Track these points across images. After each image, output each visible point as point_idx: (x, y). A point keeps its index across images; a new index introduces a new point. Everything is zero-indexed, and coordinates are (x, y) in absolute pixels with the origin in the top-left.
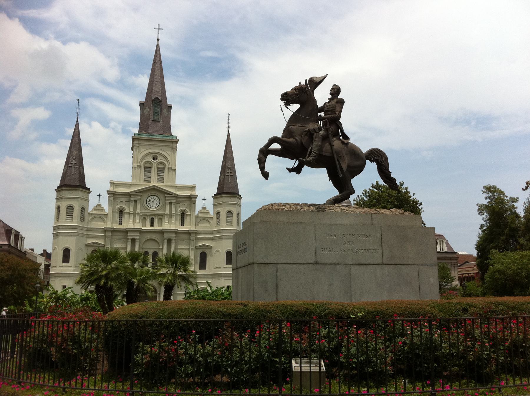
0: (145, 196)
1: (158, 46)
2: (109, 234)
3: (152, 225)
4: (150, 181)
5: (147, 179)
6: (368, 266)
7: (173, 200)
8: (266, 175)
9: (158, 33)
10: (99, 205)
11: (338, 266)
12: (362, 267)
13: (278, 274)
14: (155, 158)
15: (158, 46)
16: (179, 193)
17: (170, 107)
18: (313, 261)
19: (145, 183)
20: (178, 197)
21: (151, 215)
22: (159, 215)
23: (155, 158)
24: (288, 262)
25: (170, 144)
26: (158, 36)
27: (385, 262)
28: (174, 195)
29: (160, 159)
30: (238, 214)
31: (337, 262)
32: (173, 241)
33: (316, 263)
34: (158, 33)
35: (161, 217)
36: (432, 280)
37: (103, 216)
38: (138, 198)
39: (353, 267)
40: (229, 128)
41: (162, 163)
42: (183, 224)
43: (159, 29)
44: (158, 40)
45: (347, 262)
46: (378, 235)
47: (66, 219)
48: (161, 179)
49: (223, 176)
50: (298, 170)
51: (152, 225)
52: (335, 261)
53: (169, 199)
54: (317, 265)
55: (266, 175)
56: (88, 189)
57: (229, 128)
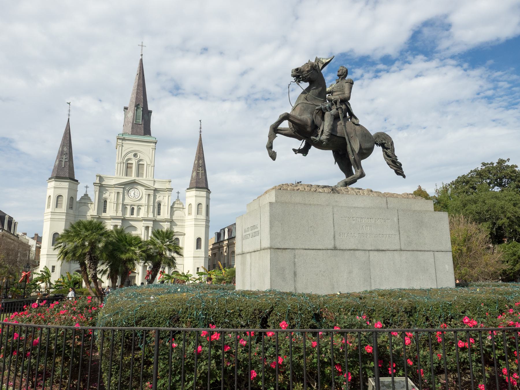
1: (141, 60)
3: (132, 214)
4: (131, 176)
6: (386, 252)
7: (152, 192)
8: (273, 156)
10: (86, 195)
11: (357, 252)
12: (381, 253)
13: (296, 260)
14: (135, 155)
15: (141, 60)
16: (157, 186)
18: (331, 246)
19: (126, 177)
20: (156, 190)
21: (131, 205)
22: (138, 206)
23: (135, 155)
24: (306, 248)
26: (142, 52)
27: (403, 248)
28: (152, 188)
30: (208, 207)
31: (356, 248)
33: (335, 249)
35: (139, 207)
36: (447, 266)
38: (121, 190)
39: (371, 252)
40: (201, 132)
42: (159, 214)
45: (366, 248)
46: (396, 219)
47: (57, 207)
49: (195, 174)
50: (304, 151)
51: (132, 214)
52: (354, 247)
54: (336, 251)
55: (273, 156)
56: (77, 181)
57: (201, 132)
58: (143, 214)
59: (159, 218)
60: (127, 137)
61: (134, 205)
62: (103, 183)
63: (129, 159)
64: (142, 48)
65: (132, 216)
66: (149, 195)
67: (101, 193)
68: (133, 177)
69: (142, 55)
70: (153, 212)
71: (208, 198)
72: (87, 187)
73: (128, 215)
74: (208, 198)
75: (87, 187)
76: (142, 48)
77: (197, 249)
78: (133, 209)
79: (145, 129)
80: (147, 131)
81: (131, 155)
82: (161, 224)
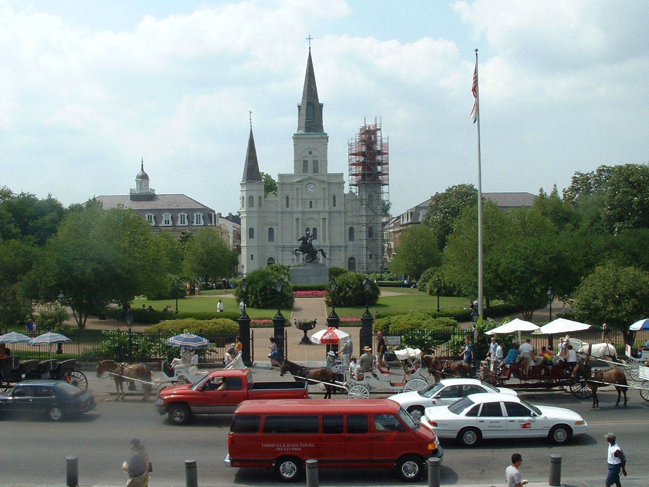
0: (306, 183)
2: (280, 215)
3: (311, 207)
5: (305, 169)
7: (326, 186)
9: (310, 43)
14: (310, 153)
17: (321, 106)
19: (305, 174)
20: (329, 183)
22: (315, 200)
23: (310, 153)
25: (322, 140)
29: (314, 153)
32: (327, 220)
34: (310, 43)
37: (275, 202)
38: (299, 186)
41: (314, 156)
42: (334, 206)
43: (310, 39)
44: (310, 48)
48: (315, 170)
51: (311, 207)
53: (323, 186)
58: (320, 207)
61: (312, 199)
64: (310, 41)
65: (311, 210)
69: (310, 48)
73: (308, 209)
76: (310, 41)
78: (311, 202)
81: (306, 153)
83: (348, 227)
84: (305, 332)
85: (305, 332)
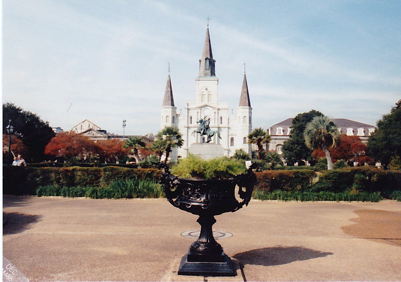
7: (216, 111)
14: (206, 89)
20: (219, 109)
38: (199, 111)
42: (221, 123)
59: (221, 126)
60: (201, 79)
62: (189, 107)
63: (203, 92)
66: (215, 112)
67: (188, 112)
68: (205, 103)
70: (218, 123)
71: (250, 113)
72: (181, 110)
74: (250, 113)
75: (181, 110)
77: (244, 144)
79: (211, 72)
80: (213, 73)
81: (204, 90)
82: (222, 129)
83: (230, 137)
84: (206, 224)
85: (206, 224)
